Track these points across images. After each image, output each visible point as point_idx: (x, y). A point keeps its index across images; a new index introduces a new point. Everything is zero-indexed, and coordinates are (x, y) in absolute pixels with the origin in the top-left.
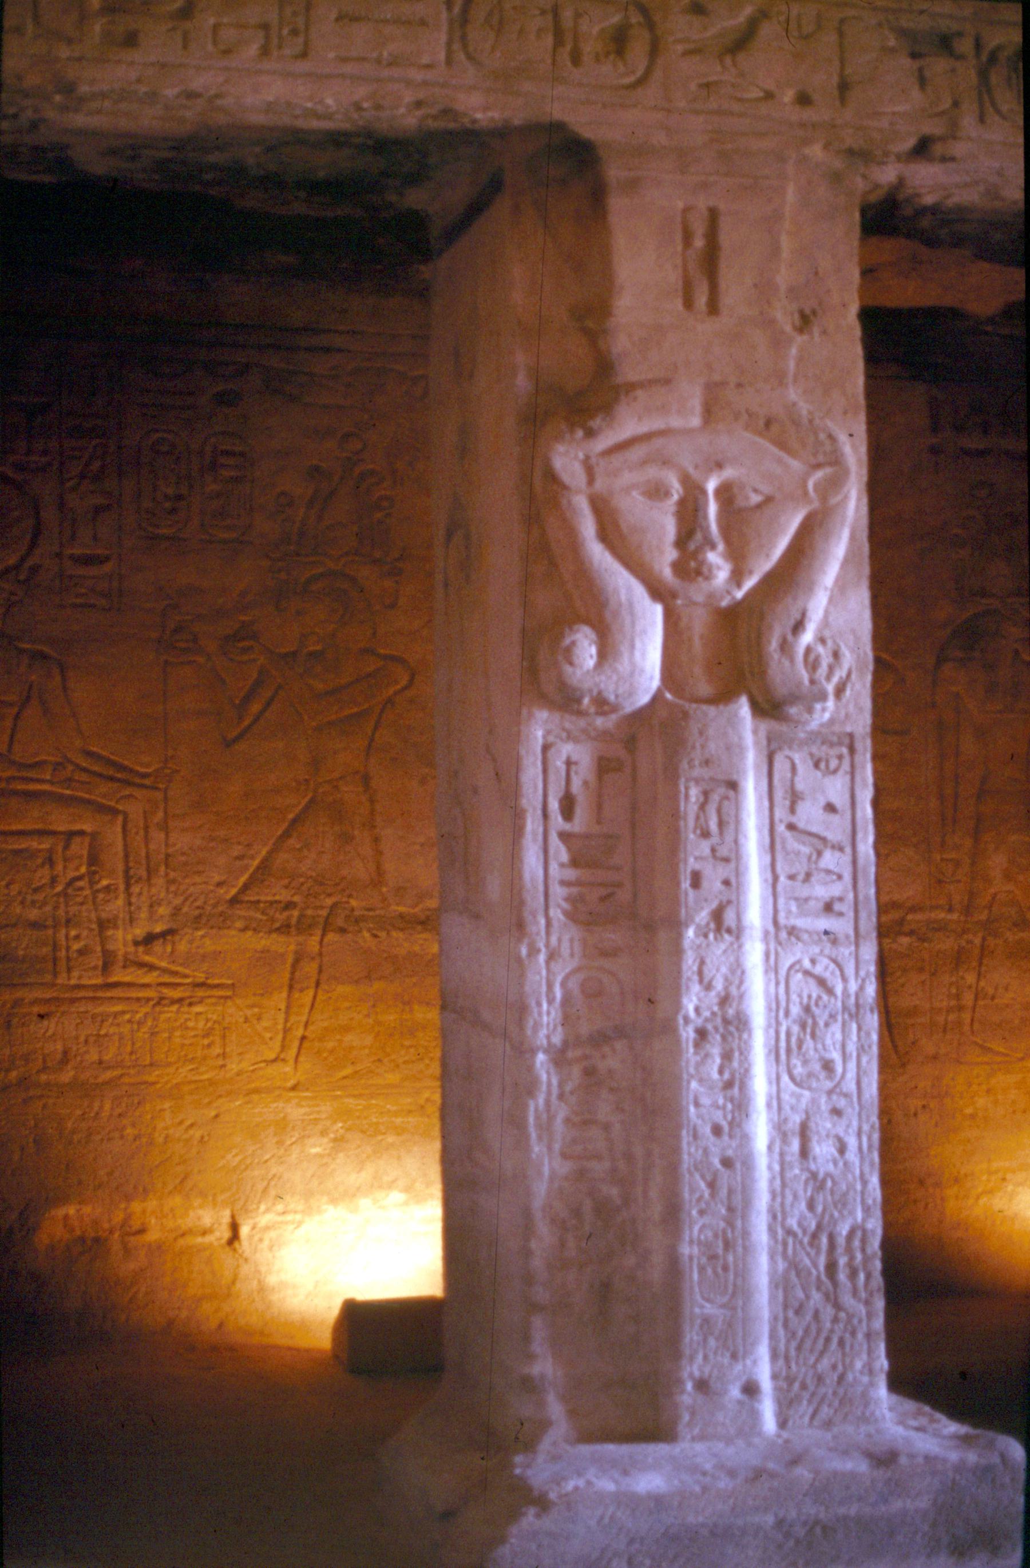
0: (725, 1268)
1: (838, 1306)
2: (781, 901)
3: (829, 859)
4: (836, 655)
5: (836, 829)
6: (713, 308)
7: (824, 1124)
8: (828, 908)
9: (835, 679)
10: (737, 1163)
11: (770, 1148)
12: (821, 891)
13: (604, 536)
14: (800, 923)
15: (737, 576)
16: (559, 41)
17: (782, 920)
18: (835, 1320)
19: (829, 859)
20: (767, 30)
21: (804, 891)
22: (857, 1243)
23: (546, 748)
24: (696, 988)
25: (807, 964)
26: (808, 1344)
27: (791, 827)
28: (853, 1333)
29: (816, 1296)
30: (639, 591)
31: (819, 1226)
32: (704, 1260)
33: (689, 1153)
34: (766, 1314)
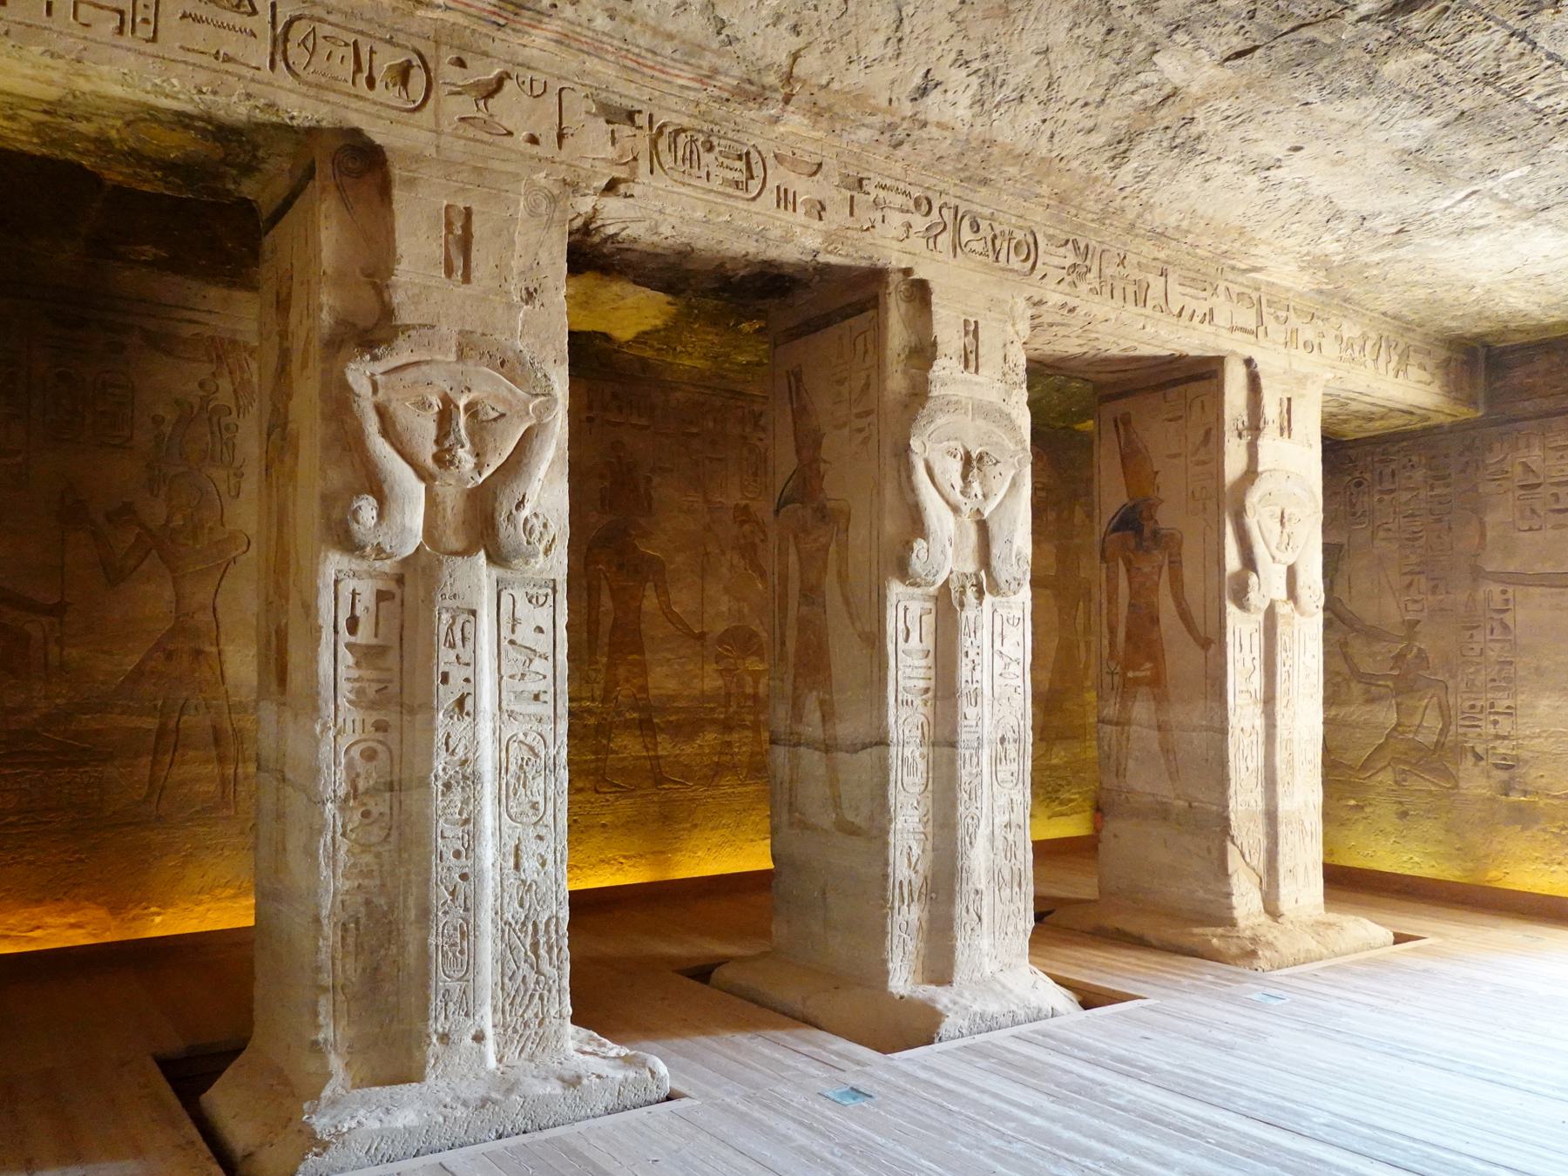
0: (462, 952)
1: (538, 972)
2: (504, 694)
3: (538, 664)
4: (545, 526)
5: (543, 644)
6: (467, 279)
7: (531, 847)
9: (544, 543)
12: (533, 686)
14: (516, 708)
15: (479, 468)
16: (358, 67)
18: (537, 982)
19: (538, 664)
20: (509, 85)
21: (520, 686)
22: (553, 927)
24: (443, 753)
25: (521, 737)
26: (518, 1000)
27: (512, 642)
29: (525, 967)
32: (446, 947)
33: (437, 870)
34: (489, 981)
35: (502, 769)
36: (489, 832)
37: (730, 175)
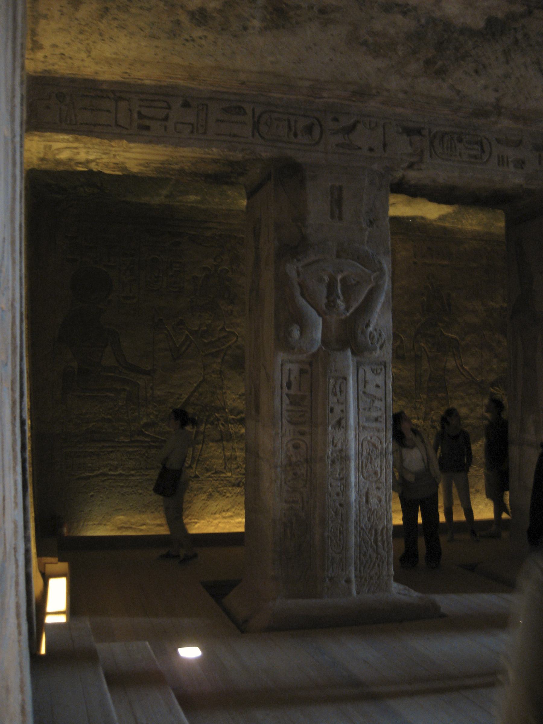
0: (340, 540)
2: (360, 418)
3: (377, 404)
4: (380, 335)
5: (380, 393)
6: (340, 218)
7: (374, 492)
8: (376, 420)
9: (380, 343)
10: (345, 505)
11: (355, 500)
12: (375, 414)
13: (302, 295)
14: (366, 424)
15: (347, 309)
17: (361, 423)
18: (377, 558)
19: (377, 404)
20: (359, 127)
22: (385, 532)
23: (282, 365)
24: (331, 446)
25: (369, 438)
28: (383, 562)
30: (314, 313)
31: (372, 526)
32: (333, 538)
35: (359, 454)
36: (353, 484)
37: (473, 153)
